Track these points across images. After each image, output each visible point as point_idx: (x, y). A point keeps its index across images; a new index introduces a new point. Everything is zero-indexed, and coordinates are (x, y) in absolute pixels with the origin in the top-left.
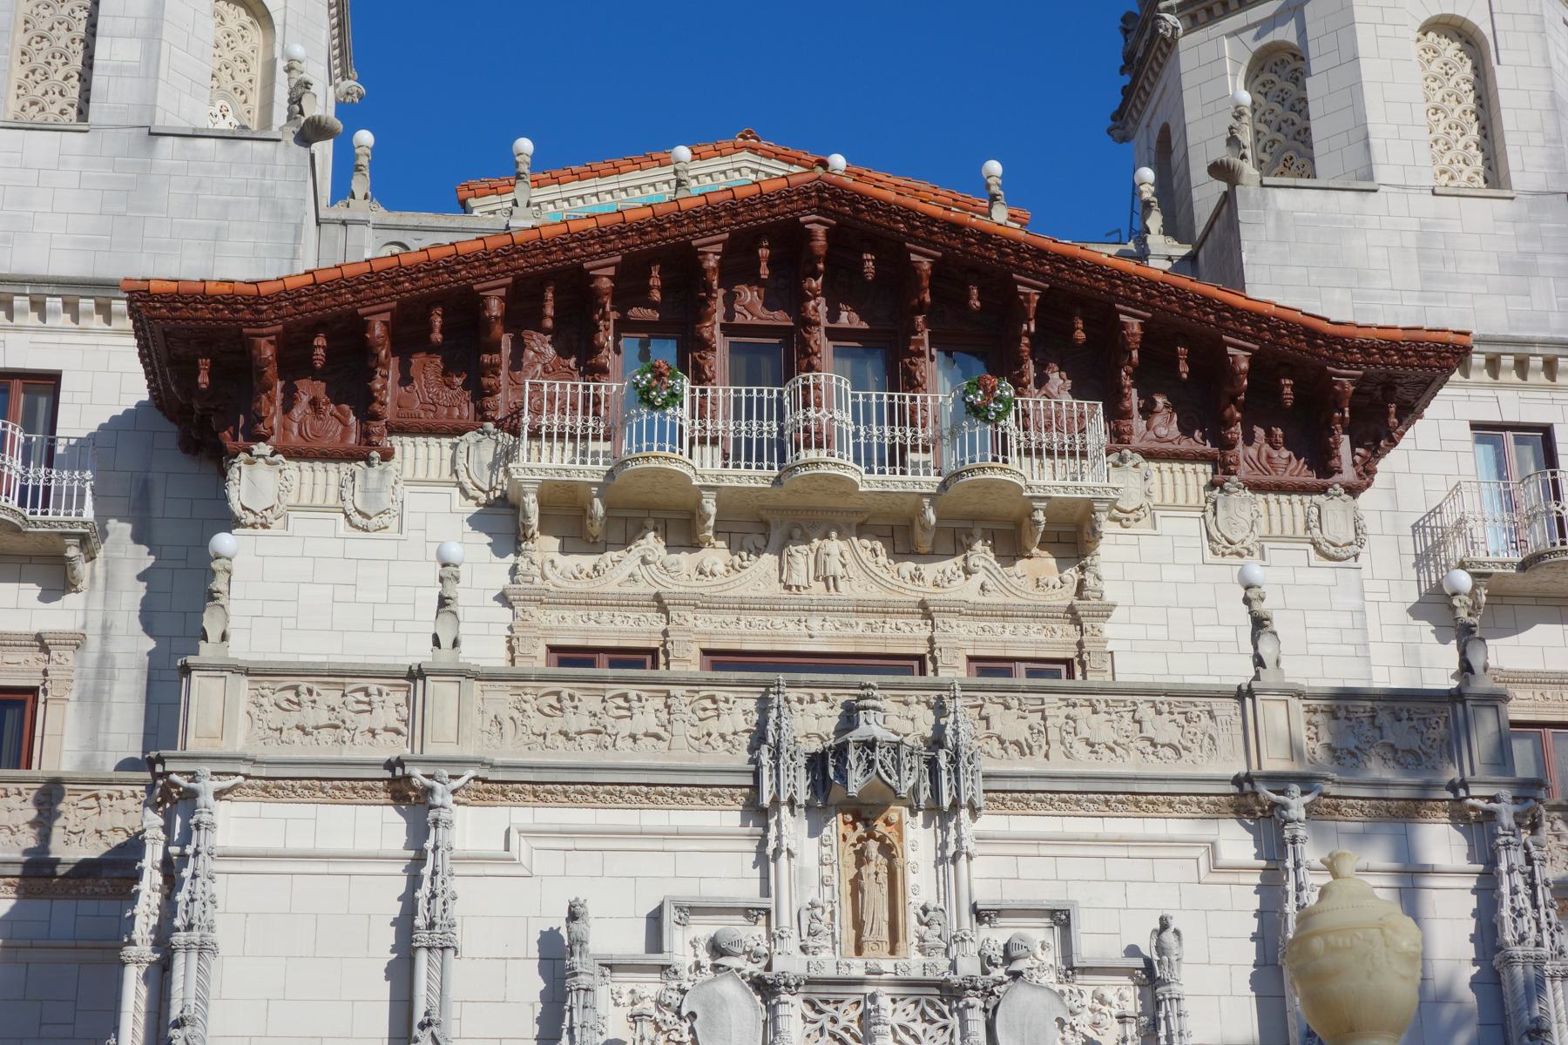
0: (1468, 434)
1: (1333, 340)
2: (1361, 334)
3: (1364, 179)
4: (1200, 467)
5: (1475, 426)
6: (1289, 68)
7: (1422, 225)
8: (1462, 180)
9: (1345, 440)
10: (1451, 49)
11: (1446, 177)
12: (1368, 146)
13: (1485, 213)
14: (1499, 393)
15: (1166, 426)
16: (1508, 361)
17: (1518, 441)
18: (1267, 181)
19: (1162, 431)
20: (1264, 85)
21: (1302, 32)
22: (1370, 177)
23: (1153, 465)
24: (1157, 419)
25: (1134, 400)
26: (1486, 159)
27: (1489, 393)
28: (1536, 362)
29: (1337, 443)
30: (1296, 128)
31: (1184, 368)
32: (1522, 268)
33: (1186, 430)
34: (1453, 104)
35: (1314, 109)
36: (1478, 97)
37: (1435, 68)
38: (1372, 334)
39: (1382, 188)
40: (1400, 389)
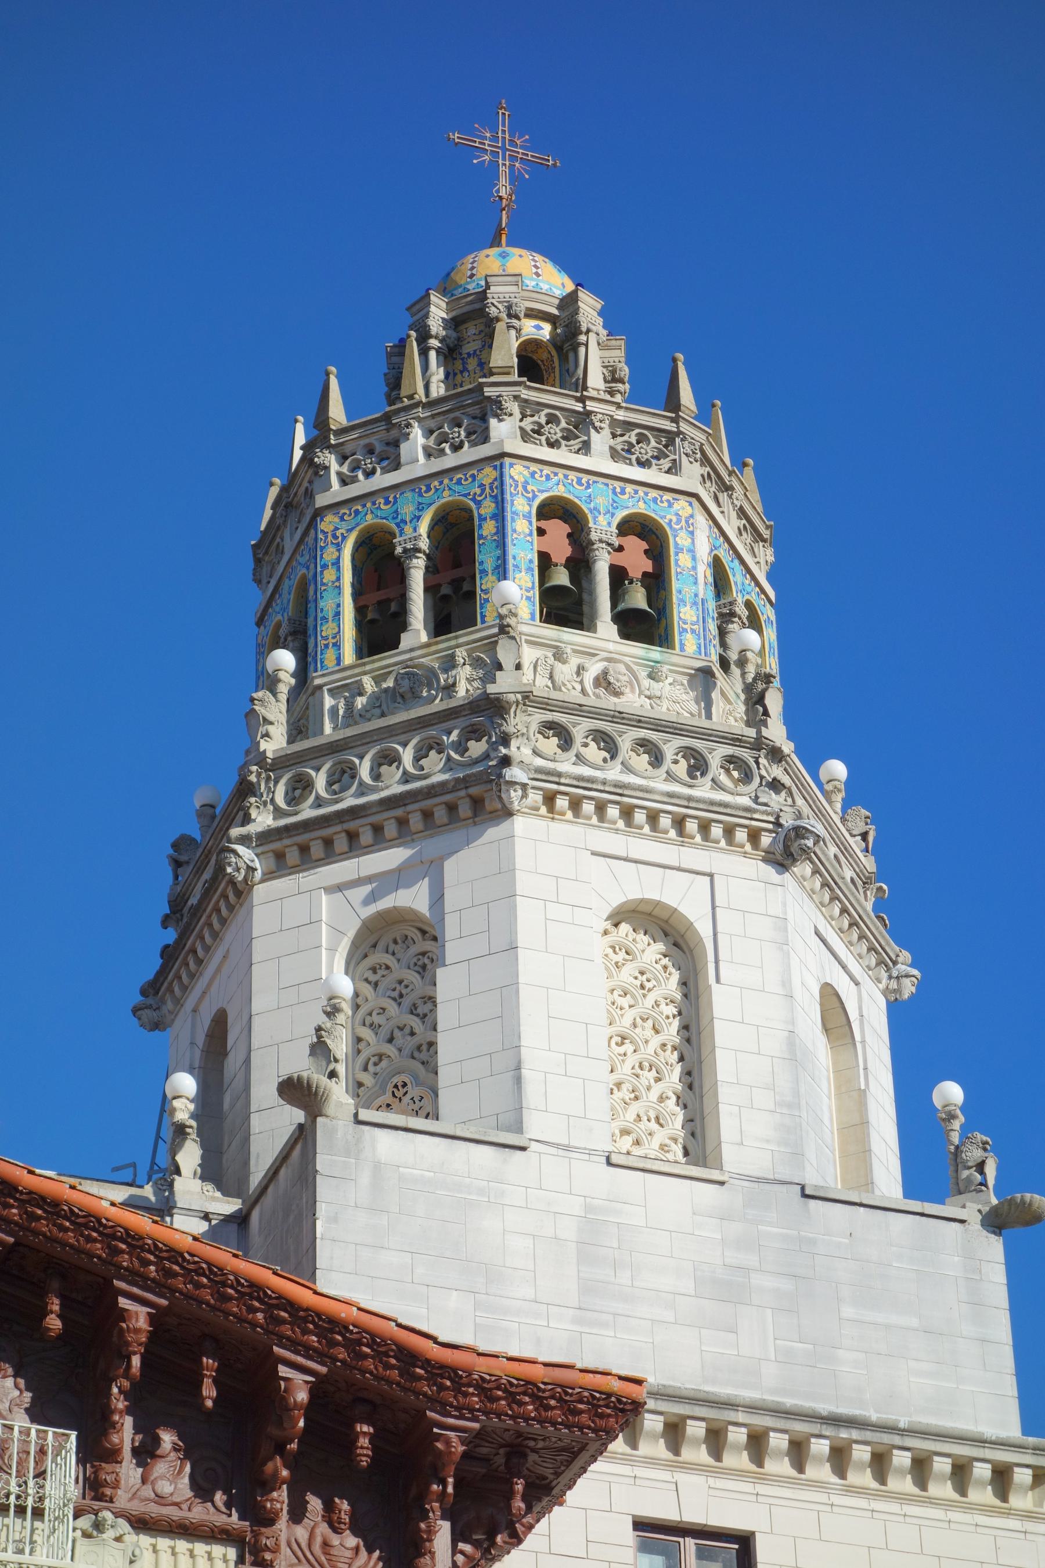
0: (629, 1536)
1: (438, 1371)
2: (482, 1366)
3: (509, 1129)
4: (218, 1550)
5: (640, 1525)
6: (414, 950)
7: (588, 1208)
8: (651, 1147)
9: (444, 1530)
10: (651, 952)
11: (628, 1140)
12: (518, 1080)
13: (678, 1200)
14: (681, 1477)
15: (172, 1480)
16: (696, 1429)
17: (702, 1554)
18: (365, 1115)
19: (165, 1488)
20: (374, 970)
21: (437, 899)
22: (518, 1127)
23: (145, 1540)
24: (160, 1468)
25: (126, 1433)
26: (689, 1121)
27: (666, 1475)
28: (737, 1436)
29: (431, 1532)
30: (416, 1040)
31: (209, 1391)
32: (728, 1290)
33: (202, 1490)
34: (649, 1032)
35: (444, 1015)
36: (685, 1027)
37: (627, 975)
38: (500, 1368)
39: (534, 1146)
40: (533, 1457)
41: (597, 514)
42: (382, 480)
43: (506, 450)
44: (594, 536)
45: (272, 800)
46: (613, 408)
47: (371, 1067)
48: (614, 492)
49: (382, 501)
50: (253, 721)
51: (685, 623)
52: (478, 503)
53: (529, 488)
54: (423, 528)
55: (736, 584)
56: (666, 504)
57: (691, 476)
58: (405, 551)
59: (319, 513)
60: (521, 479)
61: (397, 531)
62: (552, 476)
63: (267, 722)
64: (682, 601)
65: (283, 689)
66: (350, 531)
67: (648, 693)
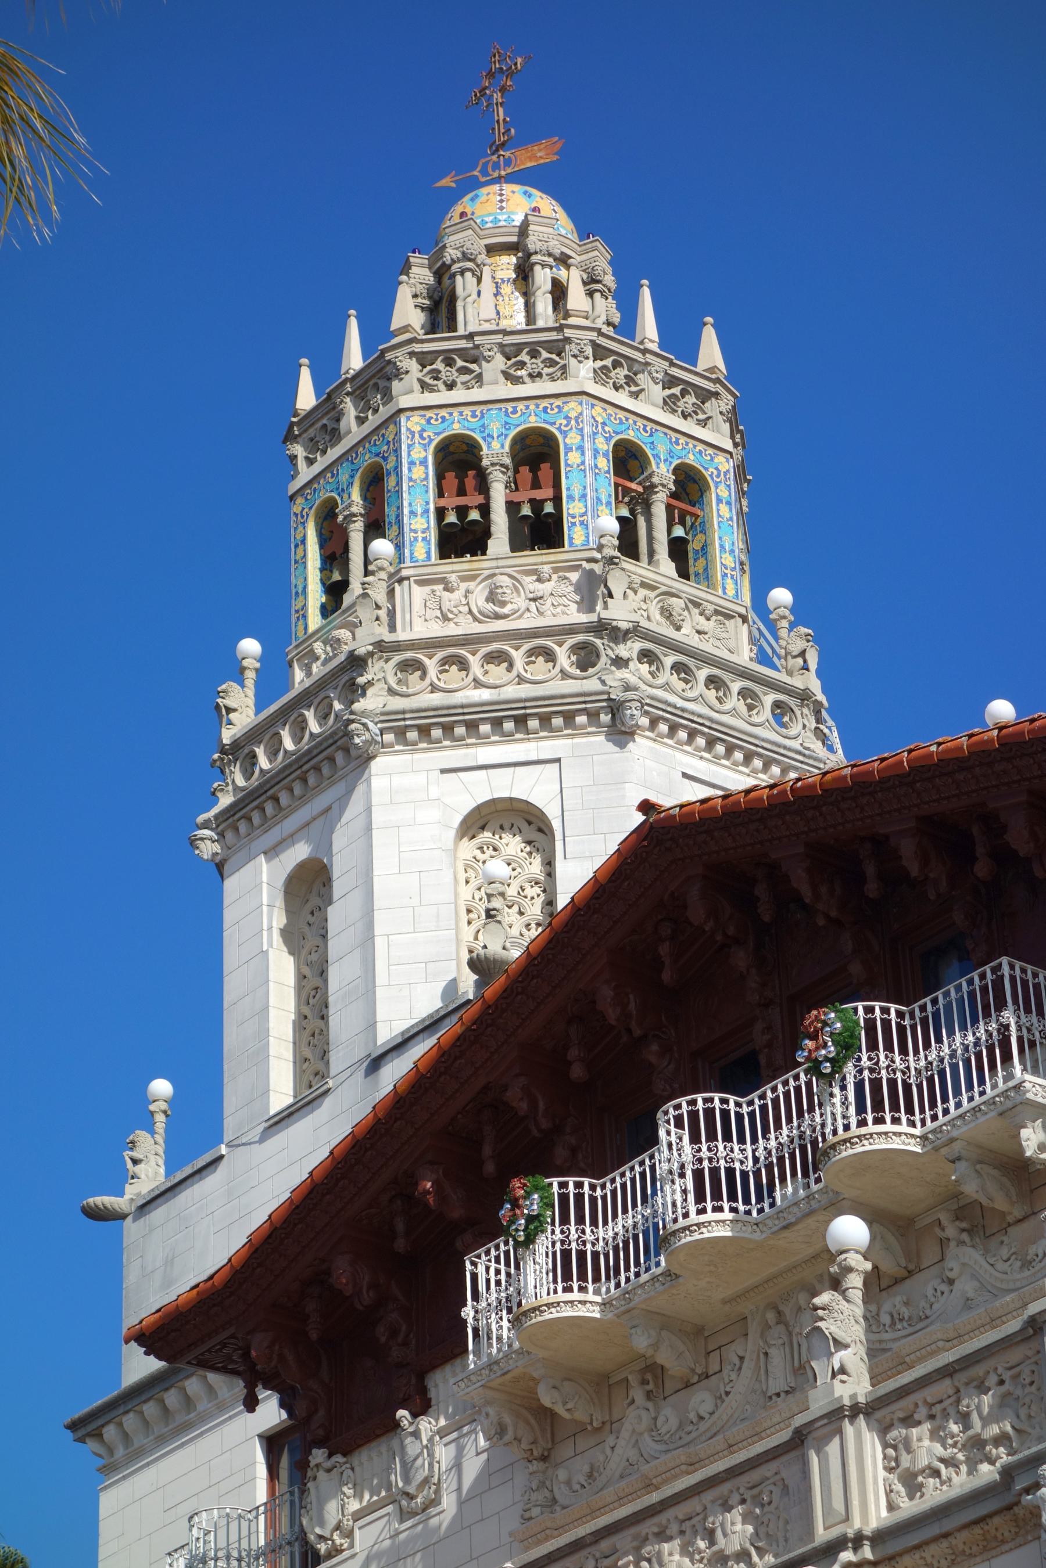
41: (489, 439)
42: (333, 453)
43: (401, 406)
44: (485, 462)
45: (233, 781)
46: (501, 336)
47: (311, 1001)
48: (507, 415)
49: (329, 475)
50: (221, 714)
51: (574, 517)
52: (385, 459)
53: (425, 435)
54: (356, 496)
55: (656, 456)
56: (556, 410)
57: (583, 374)
58: (346, 517)
59: (292, 498)
60: (417, 429)
61: (339, 502)
62: (447, 416)
63: (229, 710)
64: (571, 498)
65: (250, 676)
66: (311, 508)
67: (531, 596)
